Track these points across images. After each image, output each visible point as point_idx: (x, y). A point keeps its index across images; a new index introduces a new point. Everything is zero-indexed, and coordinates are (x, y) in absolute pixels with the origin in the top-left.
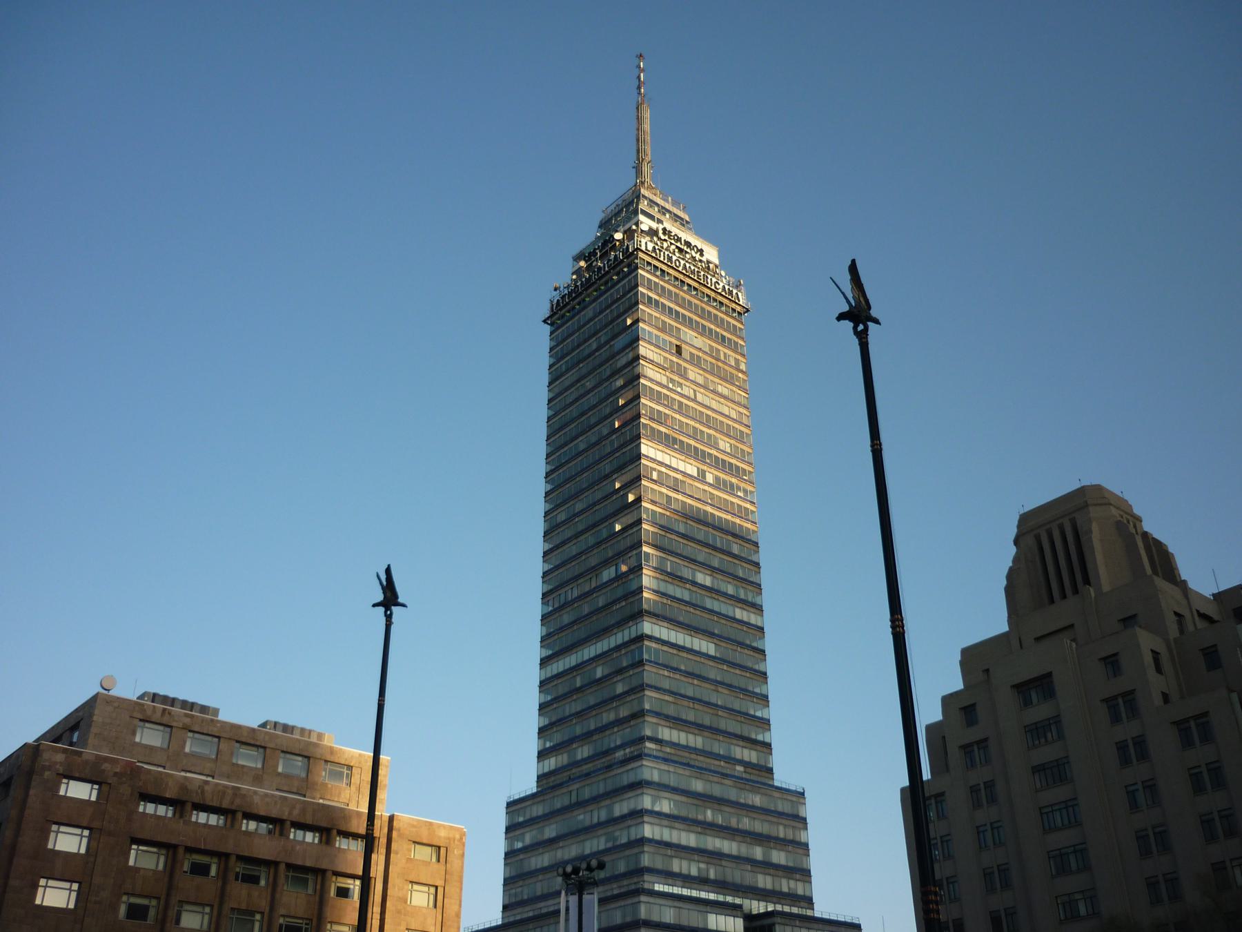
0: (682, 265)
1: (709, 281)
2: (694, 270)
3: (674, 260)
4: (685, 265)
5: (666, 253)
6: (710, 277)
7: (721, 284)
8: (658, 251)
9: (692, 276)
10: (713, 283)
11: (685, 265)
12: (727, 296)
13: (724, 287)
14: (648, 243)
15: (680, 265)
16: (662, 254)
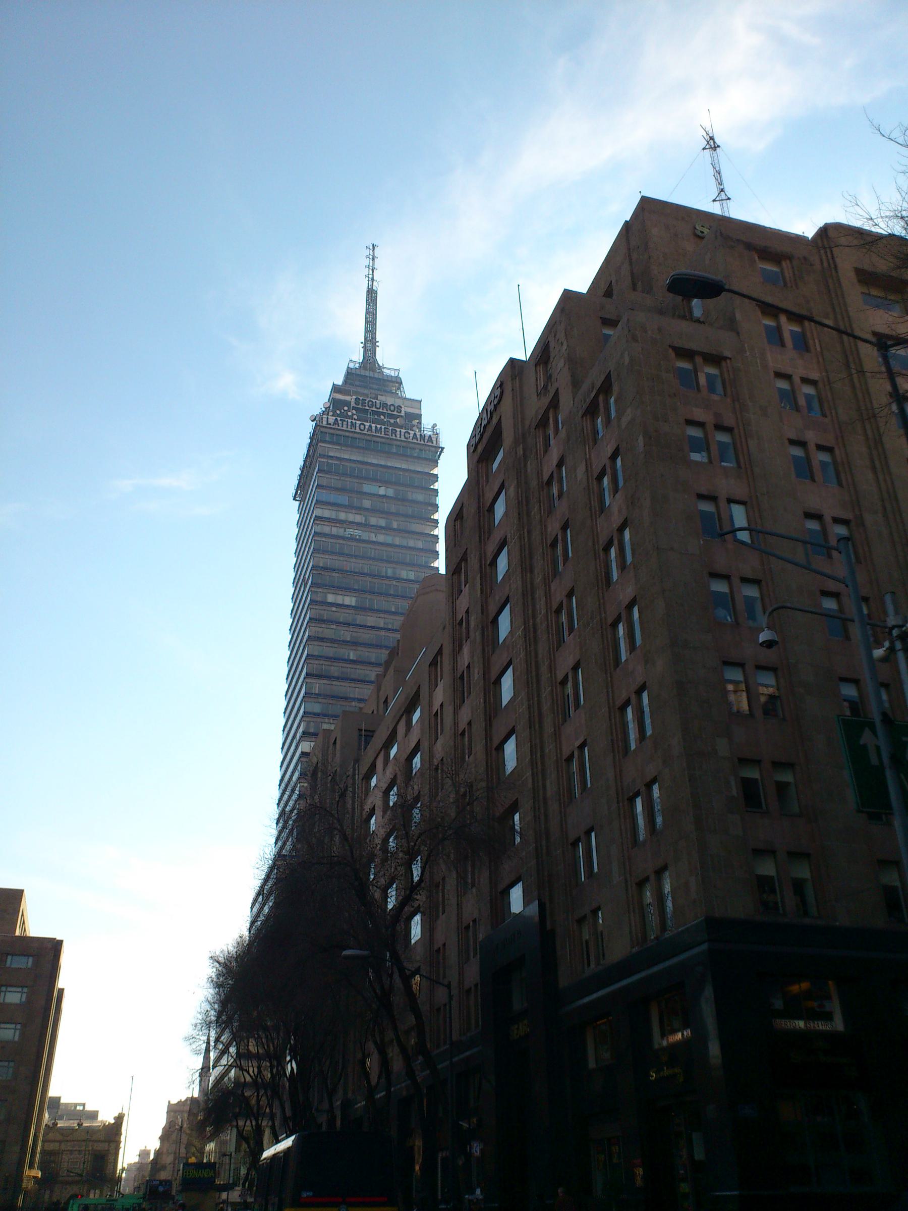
0: (367, 427)
1: (398, 433)
2: (381, 427)
3: (357, 425)
4: (370, 426)
5: (350, 421)
6: (398, 430)
7: (412, 433)
8: (340, 422)
9: (379, 435)
10: (403, 434)
11: (370, 426)
12: (419, 442)
13: (415, 434)
14: (329, 417)
15: (365, 428)
16: (345, 423)
